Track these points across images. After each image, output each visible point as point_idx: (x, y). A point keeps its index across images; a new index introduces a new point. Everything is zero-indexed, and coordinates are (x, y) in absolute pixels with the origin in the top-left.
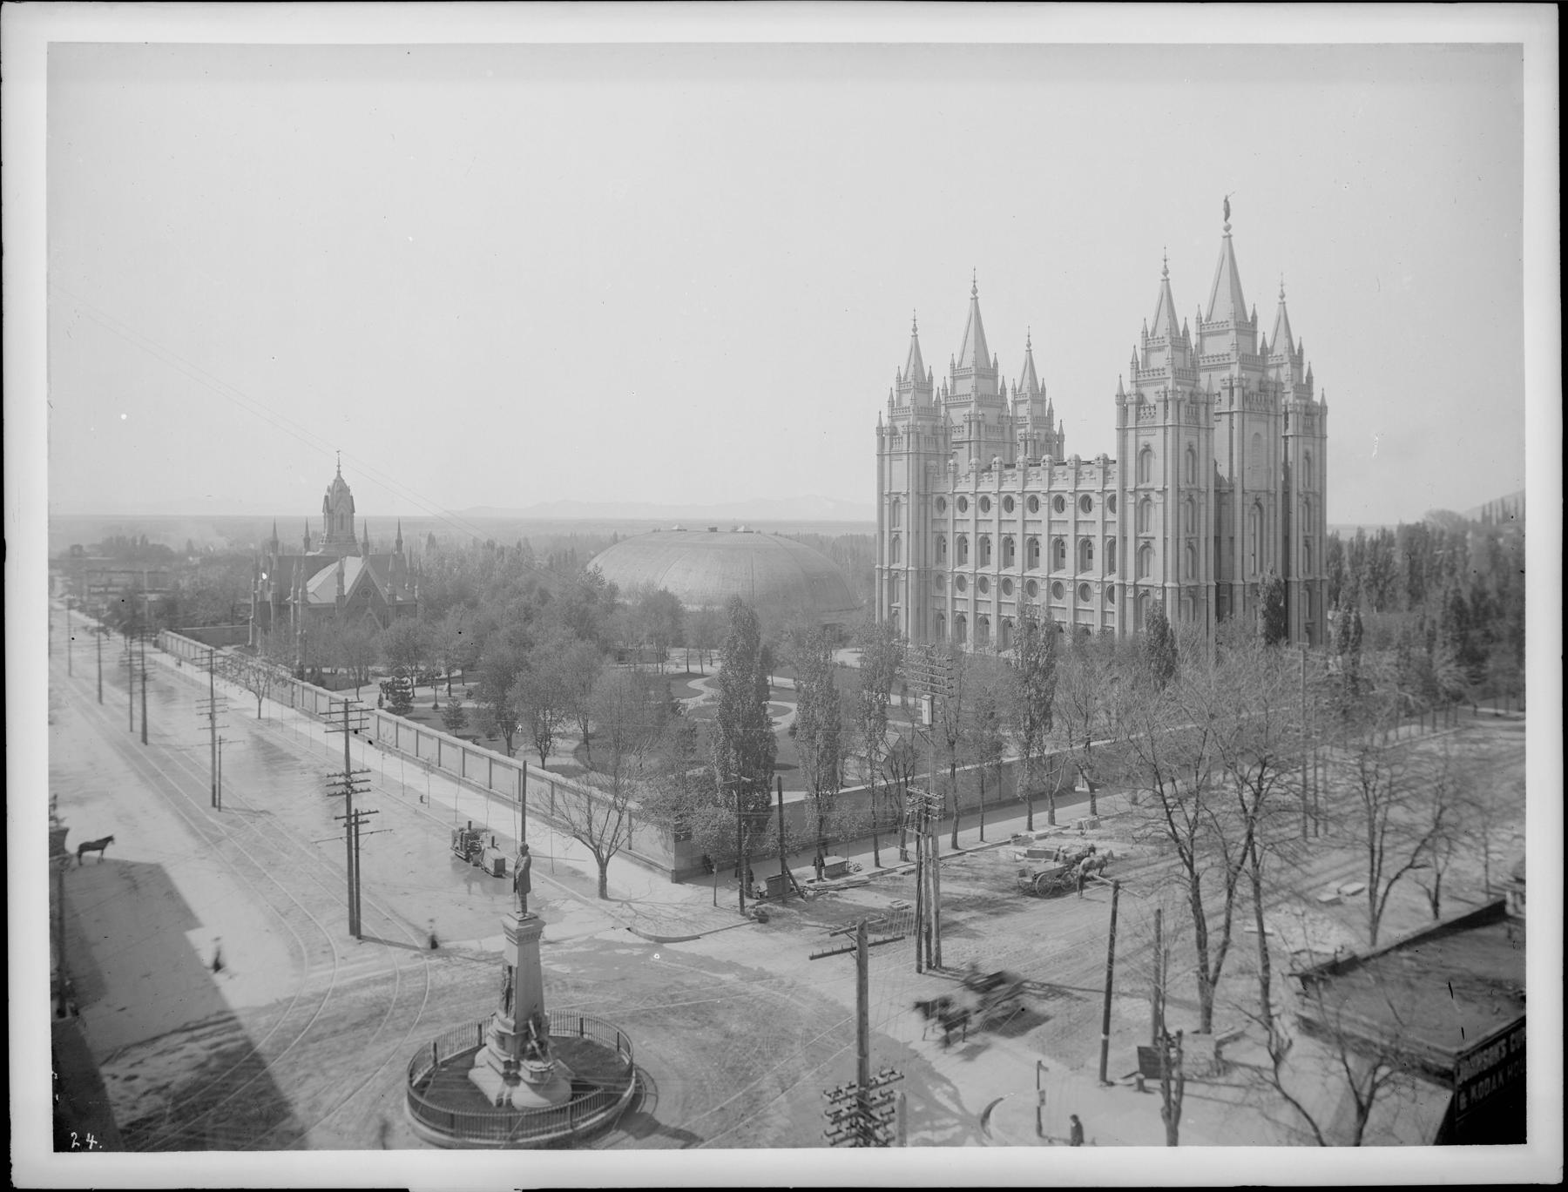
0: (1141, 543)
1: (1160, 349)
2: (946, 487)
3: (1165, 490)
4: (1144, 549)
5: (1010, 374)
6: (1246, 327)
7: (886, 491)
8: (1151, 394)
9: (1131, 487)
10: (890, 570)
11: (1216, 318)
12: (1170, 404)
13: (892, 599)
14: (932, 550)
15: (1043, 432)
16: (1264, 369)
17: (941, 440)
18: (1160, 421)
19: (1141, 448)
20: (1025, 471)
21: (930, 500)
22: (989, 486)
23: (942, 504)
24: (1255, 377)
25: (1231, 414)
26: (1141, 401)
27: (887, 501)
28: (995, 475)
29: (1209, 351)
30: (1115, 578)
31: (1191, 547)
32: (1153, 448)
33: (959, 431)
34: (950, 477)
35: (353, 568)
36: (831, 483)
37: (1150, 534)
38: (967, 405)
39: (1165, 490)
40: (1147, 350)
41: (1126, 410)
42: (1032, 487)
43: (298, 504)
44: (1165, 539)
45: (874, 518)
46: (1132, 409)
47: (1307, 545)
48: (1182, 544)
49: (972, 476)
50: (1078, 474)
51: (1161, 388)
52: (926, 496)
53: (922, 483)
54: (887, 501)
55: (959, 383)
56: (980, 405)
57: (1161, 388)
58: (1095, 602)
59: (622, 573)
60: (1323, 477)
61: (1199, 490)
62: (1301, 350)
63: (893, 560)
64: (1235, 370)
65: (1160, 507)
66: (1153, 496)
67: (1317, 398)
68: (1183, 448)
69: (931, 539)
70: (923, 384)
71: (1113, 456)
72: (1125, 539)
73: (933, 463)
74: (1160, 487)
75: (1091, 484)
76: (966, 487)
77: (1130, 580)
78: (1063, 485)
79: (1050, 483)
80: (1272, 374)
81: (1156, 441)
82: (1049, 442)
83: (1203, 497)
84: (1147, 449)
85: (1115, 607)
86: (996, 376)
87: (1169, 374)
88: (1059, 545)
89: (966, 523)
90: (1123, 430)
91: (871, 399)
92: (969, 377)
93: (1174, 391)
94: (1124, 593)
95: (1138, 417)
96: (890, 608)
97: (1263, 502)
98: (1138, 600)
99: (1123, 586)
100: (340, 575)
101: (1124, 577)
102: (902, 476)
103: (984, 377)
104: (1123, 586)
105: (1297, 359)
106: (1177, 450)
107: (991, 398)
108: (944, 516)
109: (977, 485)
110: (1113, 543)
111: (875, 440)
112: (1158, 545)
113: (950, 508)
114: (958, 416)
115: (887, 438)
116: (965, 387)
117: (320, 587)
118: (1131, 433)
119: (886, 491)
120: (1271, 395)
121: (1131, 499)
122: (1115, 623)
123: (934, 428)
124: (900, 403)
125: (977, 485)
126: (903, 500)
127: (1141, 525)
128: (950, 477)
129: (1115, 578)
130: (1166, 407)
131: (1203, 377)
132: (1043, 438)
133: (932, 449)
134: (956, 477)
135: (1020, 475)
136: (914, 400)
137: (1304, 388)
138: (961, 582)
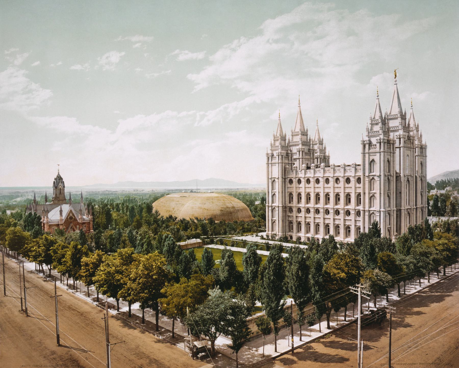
0: (371, 195)
1: (377, 124)
2: (292, 175)
3: (380, 175)
4: (372, 198)
5: (312, 135)
6: (304, 133)
7: (270, 177)
8: (374, 140)
9: (367, 174)
10: (272, 206)
11: (296, 131)
12: (382, 144)
13: (273, 217)
14: (287, 199)
15: (323, 155)
16: (309, 146)
17: (290, 158)
18: (378, 149)
19: (371, 160)
20: (324, 169)
21: (287, 180)
22: (310, 174)
23: (291, 181)
24: (306, 148)
25: (299, 159)
26: (370, 144)
27: (270, 181)
28: (312, 171)
29: (294, 140)
30: (361, 208)
31: (388, 196)
32: (375, 160)
33: (299, 154)
34: (294, 171)
35: (66, 208)
36: (253, 174)
37: (374, 192)
38: (298, 145)
39: (380, 175)
40: (372, 124)
41: (268, 158)
42: (318, 175)
43: (45, 184)
44: (380, 193)
45: (266, 186)
46: (367, 146)
47: (421, 195)
48: (386, 195)
49: (303, 171)
50: (345, 170)
51: (378, 138)
52: (285, 179)
53: (284, 174)
54: (270, 181)
55: (295, 137)
56: (303, 145)
57: (378, 138)
58: (352, 217)
59: (162, 208)
60: (426, 171)
61: (391, 175)
62: (418, 126)
63: (273, 202)
64: (300, 146)
65: (378, 182)
66: (376, 178)
67: (327, 154)
68: (386, 160)
69: (287, 195)
70: (283, 138)
71: (360, 162)
72: (364, 193)
73: (288, 166)
74: (378, 174)
75: (351, 173)
76: (301, 175)
77: (367, 208)
78: (329, 174)
79: (334, 173)
80: (411, 133)
81: (377, 158)
82: (325, 159)
83: (392, 178)
84: (373, 161)
85: (361, 218)
86: (307, 135)
87: (381, 132)
88: (327, 196)
89: (303, 188)
90: (364, 153)
91: (265, 143)
92: (396, 118)
93: (384, 139)
94: (364, 213)
95: (369, 149)
96: (272, 220)
97: (410, 179)
98: (370, 216)
99: (364, 211)
100: (61, 211)
101: (364, 208)
102: (276, 172)
103: (303, 135)
104: (364, 211)
105: (321, 143)
106: (384, 161)
107: (306, 143)
108: (292, 186)
109: (305, 174)
110: (359, 195)
111: (361, 147)
112: (377, 196)
113: (294, 183)
114: (294, 150)
115: (270, 158)
116: (298, 139)
117: (55, 216)
118: (367, 155)
119: (270, 177)
120: (412, 141)
121: (367, 179)
122: (360, 224)
123: (309, 149)
124: (274, 145)
125: (305, 174)
126: (276, 180)
127: (370, 189)
128: (294, 171)
129: (361, 208)
130: (380, 145)
131: (391, 134)
132: (323, 157)
133: (287, 161)
134: (296, 172)
135: (322, 171)
136: (281, 144)
137: (323, 151)
138: (299, 210)
